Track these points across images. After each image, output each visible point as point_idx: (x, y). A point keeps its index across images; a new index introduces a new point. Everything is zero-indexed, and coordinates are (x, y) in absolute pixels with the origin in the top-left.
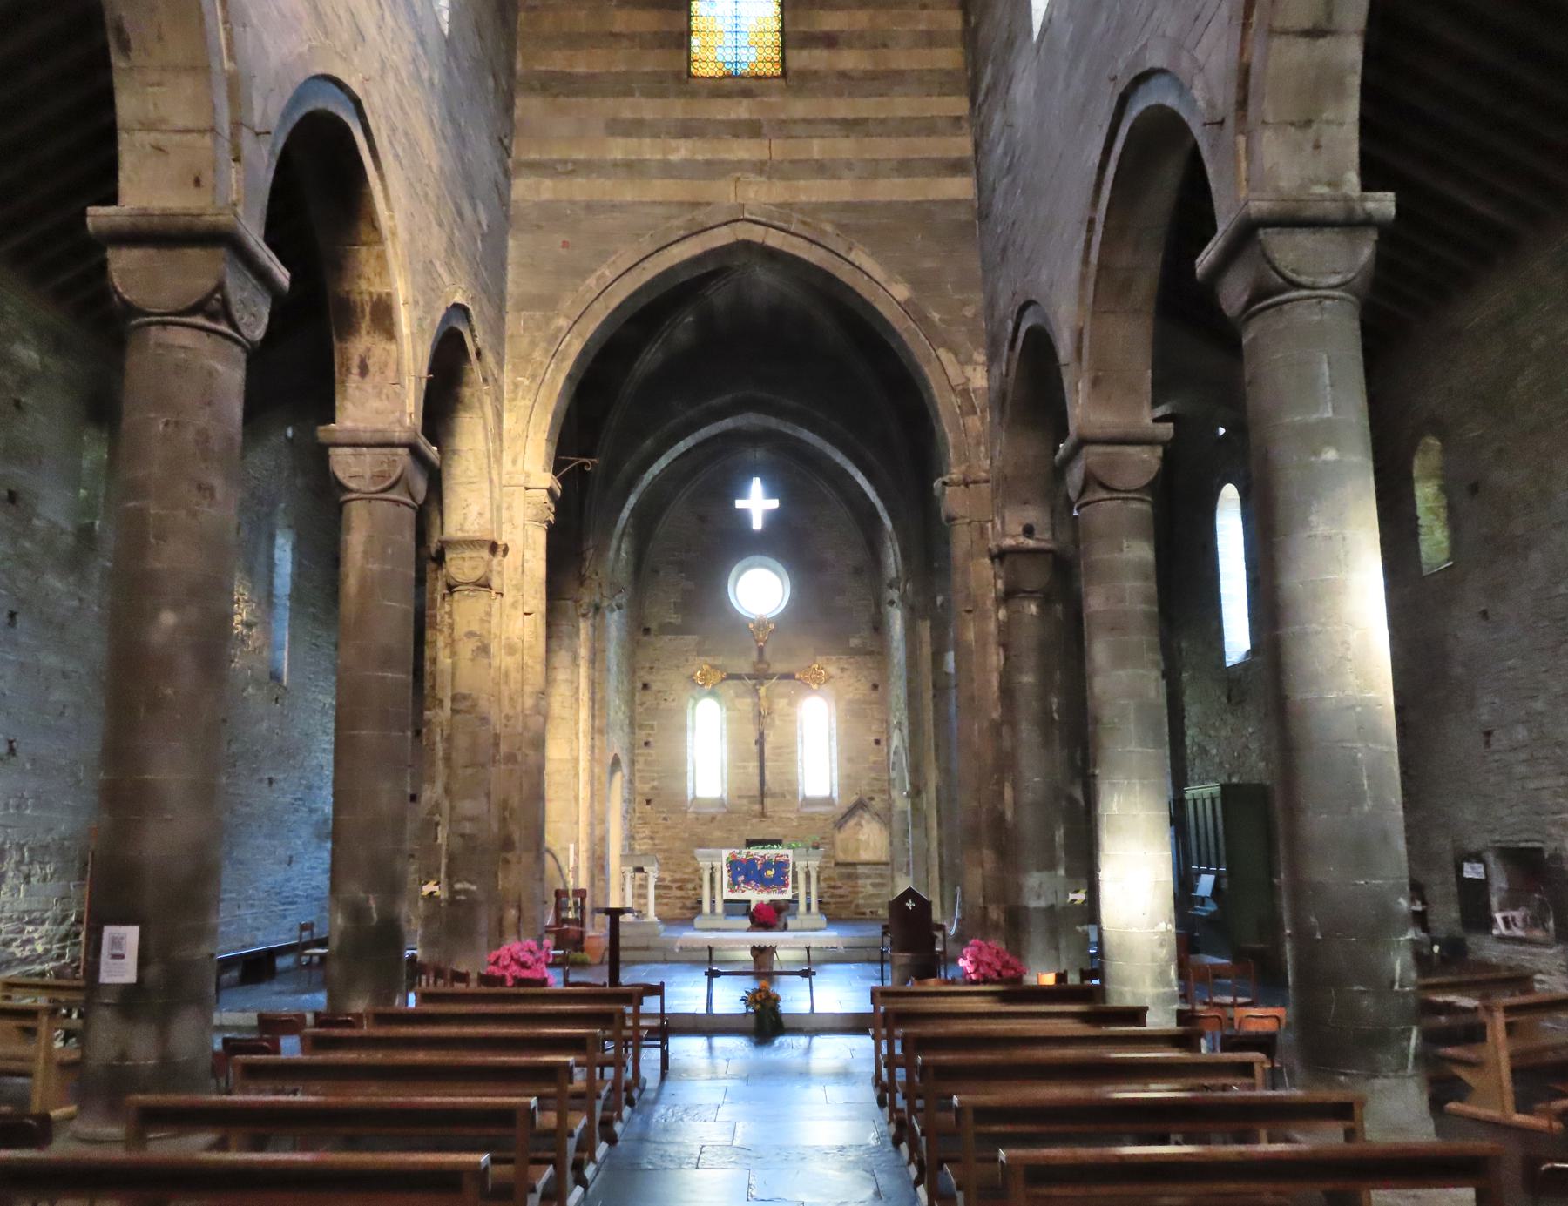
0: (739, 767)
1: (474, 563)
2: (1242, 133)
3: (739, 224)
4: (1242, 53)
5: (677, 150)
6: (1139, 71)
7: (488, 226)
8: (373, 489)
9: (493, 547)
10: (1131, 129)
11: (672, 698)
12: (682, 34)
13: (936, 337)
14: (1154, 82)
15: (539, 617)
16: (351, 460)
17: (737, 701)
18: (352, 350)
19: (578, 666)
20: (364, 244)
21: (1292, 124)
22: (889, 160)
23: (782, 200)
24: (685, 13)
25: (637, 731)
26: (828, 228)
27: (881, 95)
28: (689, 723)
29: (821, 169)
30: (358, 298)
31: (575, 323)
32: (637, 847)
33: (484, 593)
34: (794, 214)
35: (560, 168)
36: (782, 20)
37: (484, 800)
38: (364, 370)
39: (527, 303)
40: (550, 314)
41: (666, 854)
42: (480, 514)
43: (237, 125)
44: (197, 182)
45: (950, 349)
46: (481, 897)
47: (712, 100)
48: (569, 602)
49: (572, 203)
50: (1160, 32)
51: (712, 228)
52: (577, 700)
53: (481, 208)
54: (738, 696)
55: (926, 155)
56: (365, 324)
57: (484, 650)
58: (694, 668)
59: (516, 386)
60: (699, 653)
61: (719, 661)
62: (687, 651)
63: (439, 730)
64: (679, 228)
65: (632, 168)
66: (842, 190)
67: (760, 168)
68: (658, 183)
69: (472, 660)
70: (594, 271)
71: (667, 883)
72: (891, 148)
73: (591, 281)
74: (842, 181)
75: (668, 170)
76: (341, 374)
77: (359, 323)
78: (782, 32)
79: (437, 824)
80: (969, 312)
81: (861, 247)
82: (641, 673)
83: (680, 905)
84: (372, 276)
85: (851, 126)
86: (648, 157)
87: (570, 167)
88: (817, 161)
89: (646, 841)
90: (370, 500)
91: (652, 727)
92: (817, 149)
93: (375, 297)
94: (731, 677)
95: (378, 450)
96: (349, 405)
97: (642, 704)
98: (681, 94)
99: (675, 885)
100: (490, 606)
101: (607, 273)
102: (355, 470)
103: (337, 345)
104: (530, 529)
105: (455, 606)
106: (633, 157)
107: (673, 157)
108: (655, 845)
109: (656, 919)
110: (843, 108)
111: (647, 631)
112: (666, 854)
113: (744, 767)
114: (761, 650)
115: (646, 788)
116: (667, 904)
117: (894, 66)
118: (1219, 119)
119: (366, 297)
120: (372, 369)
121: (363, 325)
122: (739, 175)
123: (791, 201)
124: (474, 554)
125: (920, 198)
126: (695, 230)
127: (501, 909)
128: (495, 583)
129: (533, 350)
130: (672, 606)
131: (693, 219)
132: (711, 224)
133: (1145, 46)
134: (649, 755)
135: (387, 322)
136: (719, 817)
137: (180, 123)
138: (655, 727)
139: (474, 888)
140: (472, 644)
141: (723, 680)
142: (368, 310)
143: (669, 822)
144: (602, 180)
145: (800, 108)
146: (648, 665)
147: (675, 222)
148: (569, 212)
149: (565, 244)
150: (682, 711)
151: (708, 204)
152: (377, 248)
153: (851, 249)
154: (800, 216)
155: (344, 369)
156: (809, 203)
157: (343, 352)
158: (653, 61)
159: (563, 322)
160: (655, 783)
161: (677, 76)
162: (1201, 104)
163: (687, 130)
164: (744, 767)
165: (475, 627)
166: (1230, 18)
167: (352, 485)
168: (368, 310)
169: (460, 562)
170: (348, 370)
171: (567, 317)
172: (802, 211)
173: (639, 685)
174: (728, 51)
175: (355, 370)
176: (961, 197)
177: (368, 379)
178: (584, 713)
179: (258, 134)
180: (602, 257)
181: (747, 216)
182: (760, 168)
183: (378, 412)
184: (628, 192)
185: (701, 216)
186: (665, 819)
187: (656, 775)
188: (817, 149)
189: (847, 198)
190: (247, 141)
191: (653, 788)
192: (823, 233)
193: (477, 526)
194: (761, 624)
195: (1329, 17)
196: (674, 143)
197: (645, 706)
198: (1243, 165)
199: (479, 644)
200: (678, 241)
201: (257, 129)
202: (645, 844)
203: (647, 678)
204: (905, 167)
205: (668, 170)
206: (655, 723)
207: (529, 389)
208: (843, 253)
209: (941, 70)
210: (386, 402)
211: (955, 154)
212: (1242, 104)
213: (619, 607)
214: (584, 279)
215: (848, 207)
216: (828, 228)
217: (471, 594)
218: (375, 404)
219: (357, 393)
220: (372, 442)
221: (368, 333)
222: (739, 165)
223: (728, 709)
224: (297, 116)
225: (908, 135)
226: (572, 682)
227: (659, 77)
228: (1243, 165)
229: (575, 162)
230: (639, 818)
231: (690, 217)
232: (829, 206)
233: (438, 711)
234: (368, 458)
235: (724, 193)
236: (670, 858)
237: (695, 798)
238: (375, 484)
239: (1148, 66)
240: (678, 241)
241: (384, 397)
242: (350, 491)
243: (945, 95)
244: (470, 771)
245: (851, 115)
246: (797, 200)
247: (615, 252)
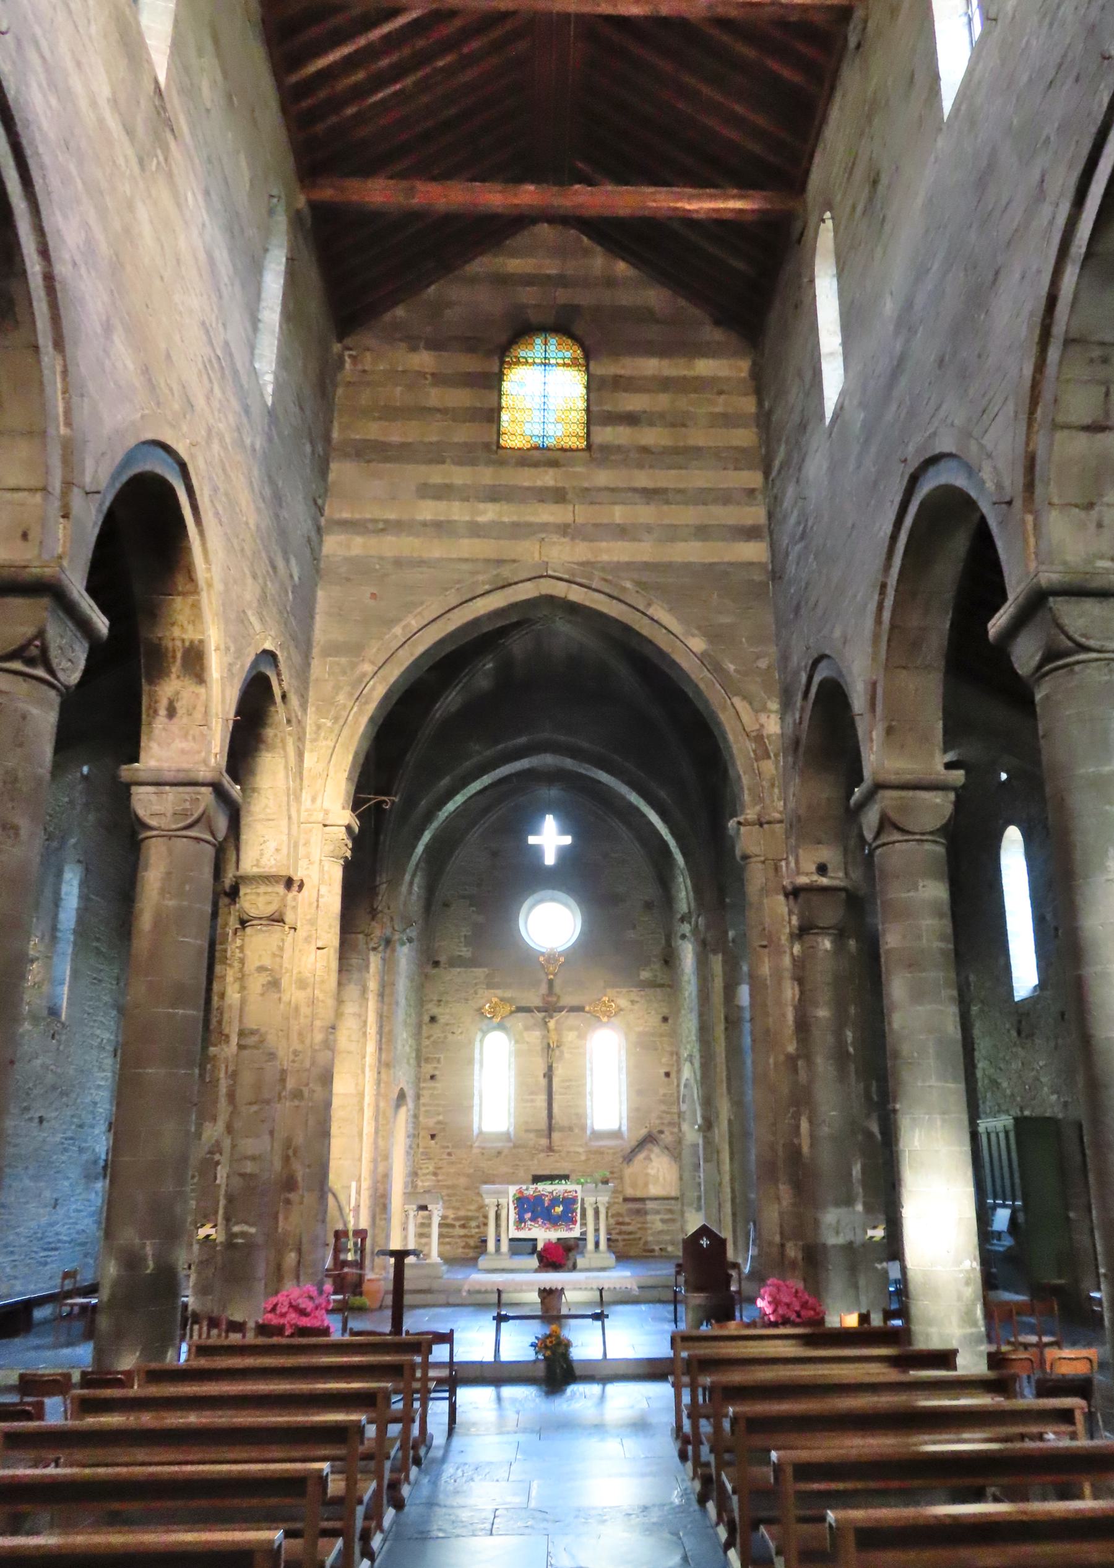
0: (527, 1101)
1: (268, 898)
2: (1031, 512)
3: (542, 580)
4: (1027, 444)
5: (484, 512)
6: (928, 455)
7: (300, 579)
8: (174, 827)
9: (289, 883)
10: (922, 504)
12: (492, 410)
13: (730, 686)
14: (943, 465)
15: (332, 951)
16: (154, 798)
17: (526, 1034)
18: (160, 693)
19: (367, 999)
20: (179, 594)
21: (1076, 506)
22: (687, 526)
23: (584, 559)
24: (496, 393)
25: (423, 1064)
26: (628, 585)
27: (681, 468)
28: (477, 1056)
29: (623, 532)
30: (170, 645)
31: (380, 668)
32: (420, 1184)
33: (277, 927)
34: (596, 573)
35: (370, 526)
36: (588, 400)
37: (266, 1138)
38: (172, 712)
39: (333, 649)
40: (354, 659)
41: (450, 1191)
42: (277, 850)
43: (68, 485)
44: (25, 536)
45: (744, 698)
46: (260, 1240)
47: (520, 469)
48: (361, 936)
49: (381, 558)
50: (949, 421)
51: (516, 583)
52: (365, 1034)
53: (293, 561)
54: (527, 1028)
55: (723, 522)
56: (176, 668)
57: (275, 984)
58: (482, 1001)
59: (319, 727)
60: (490, 986)
61: (508, 994)
62: (476, 984)
63: (223, 1067)
64: (484, 583)
65: (441, 528)
66: (643, 551)
67: (564, 530)
68: (466, 542)
69: (262, 995)
70: (400, 620)
71: (449, 1221)
72: (689, 515)
73: (398, 630)
74: (642, 544)
75: (476, 530)
76: (148, 715)
77: (169, 667)
78: (588, 410)
79: (218, 1163)
80: (763, 664)
81: (660, 603)
82: (430, 1006)
83: (463, 1244)
84: (185, 623)
85: (650, 494)
86: (456, 518)
87: (381, 526)
88: (619, 525)
89: (428, 1177)
90: (170, 837)
91: (439, 1061)
92: (618, 514)
93: (187, 644)
94: (520, 1009)
95: (181, 789)
96: (154, 746)
97: (428, 1038)
98: (489, 463)
99: (457, 1224)
100: (283, 940)
101: (413, 622)
102: (157, 808)
103: (145, 687)
104: (327, 866)
105: (247, 939)
106: (442, 518)
107: (481, 519)
108: (438, 1181)
109: (439, 1260)
110: (643, 479)
111: (436, 964)
112: (450, 1191)
113: (532, 1101)
114: (551, 983)
115: (431, 1122)
116: (449, 1243)
117: (691, 442)
118: (1007, 499)
119: (178, 643)
120: (181, 711)
121: (174, 670)
122: (543, 536)
123: (593, 560)
124: (270, 889)
125: (716, 560)
126: (501, 584)
127: (280, 1254)
128: (289, 918)
129: (337, 694)
130: (463, 939)
131: (497, 575)
132: (516, 580)
133: (935, 434)
134: (434, 1088)
135: (198, 668)
136: (506, 1152)
137: (12, 482)
138: (442, 1060)
139: (253, 1230)
140: (263, 978)
141: (512, 1012)
142: (179, 655)
143: (453, 1158)
144: (411, 538)
145: (603, 477)
147: (481, 578)
148: (377, 567)
149: (373, 596)
150: (471, 1043)
151: (514, 561)
152: (191, 599)
153: (649, 605)
154: (602, 575)
155: (151, 712)
156: (609, 563)
157: (152, 696)
158: (464, 433)
159: (368, 668)
160: (441, 1118)
161: (487, 446)
162: (990, 485)
163: (494, 495)
164: (532, 1101)
165: (267, 962)
166: (1016, 412)
167: (153, 822)
168: (179, 655)
169: (253, 897)
170: (156, 712)
171: (373, 663)
172: (603, 569)
173: (426, 1018)
174: (536, 426)
175: (163, 712)
176: (755, 560)
177: (175, 720)
178: (371, 1048)
179: (87, 493)
180: (409, 607)
181: (550, 573)
182: (564, 530)
183: (183, 752)
184: (436, 550)
185: (506, 572)
186: (449, 1154)
187: (441, 1109)
188: (618, 514)
189: (645, 559)
190: (77, 501)
191: (439, 1123)
192: (624, 589)
193: (273, 862)
194: (551, 958)
195: (1107, 413)
196: (482, 506)
197: (432, 1039)
198: (1032, 541)
199: (269, 978)
200: (483, 595)
201: (88, 489)
202: (428, 1180)
203: (435, 1011)
204: (702, 532)
205: (476, 530)
206: (442, 1056)
207: (331, 730)
208: (641, 608)
209: (736, 448)
210: (192, 744)
211: (749, 522)
212: (1029, 487)
213: (410, 940)
214: (390, 629)
215: (646, 566)
216: (628, 585)
217: (265, 928)
218: (179, 744)
219: (164, 734)
220: (175, 781)
221: (178, 677)
222: (544, 527)
223: (517, 1042)
224: (124, 478)
225: (705, 504)
226: (360, 1016)
227: (469, 447)
228: (1032, 541)
229: (386, 521)
230: (422, 1153)
231: (495, 572)
232: (629, 566)
233: (224, 1046)
234: (171, 797)
235: (528, 551)
236: (454, 1195)
237: (481, 1133)
238: (176, 822)
239: (937, 451)
240: (483, 595)
241: (190, 738)
242: (151, 828)
243: (741, 469)
244: (255, 1108)
245: (650, 484)
246: (599, 559)
247: (422, 603)
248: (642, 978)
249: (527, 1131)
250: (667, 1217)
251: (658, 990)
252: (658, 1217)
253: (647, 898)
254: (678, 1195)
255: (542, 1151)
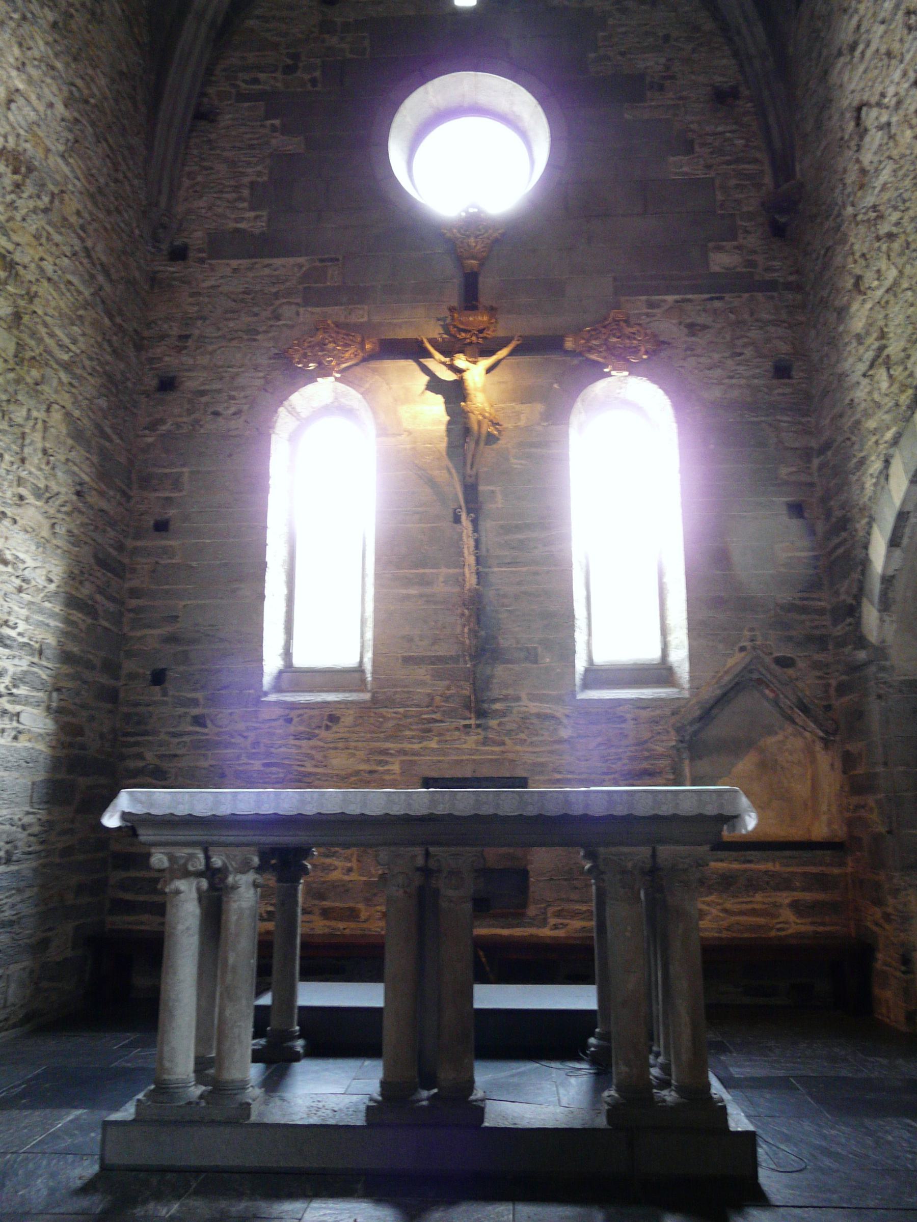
11: (233, 410)
60: (311, 297)
62: (276, 295)
111: (179, 254)
134: (166, 551)
138: (185, 478)
146: (175, 331)
203: (171, 361)
248: (715, 268)
249: (407, 660)
250: (807, 896)
251: (760, 296)
252: (785, 898)
253: (718, 79)
254: (840, 832)
255: (451, 713)
